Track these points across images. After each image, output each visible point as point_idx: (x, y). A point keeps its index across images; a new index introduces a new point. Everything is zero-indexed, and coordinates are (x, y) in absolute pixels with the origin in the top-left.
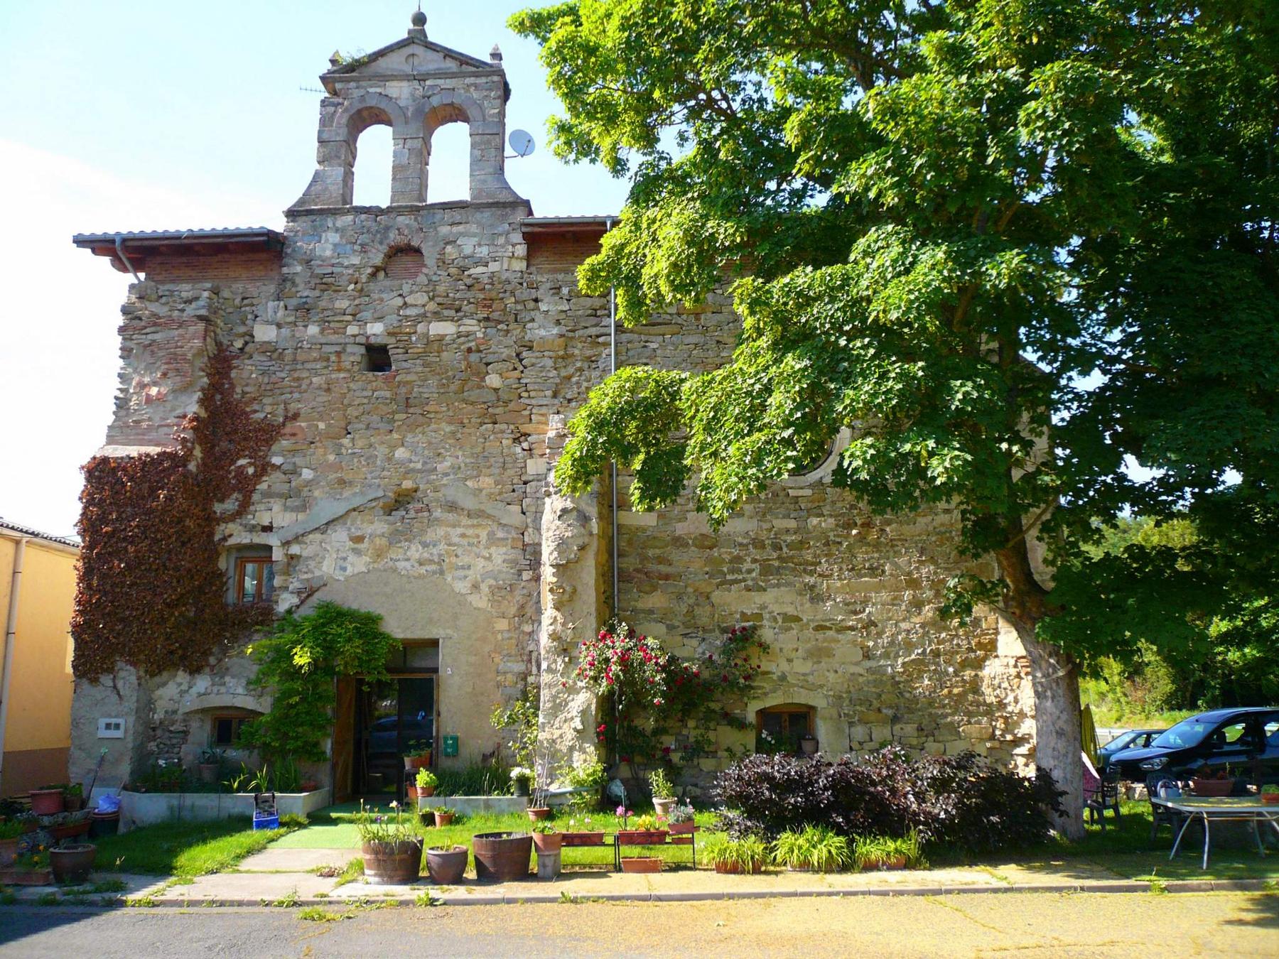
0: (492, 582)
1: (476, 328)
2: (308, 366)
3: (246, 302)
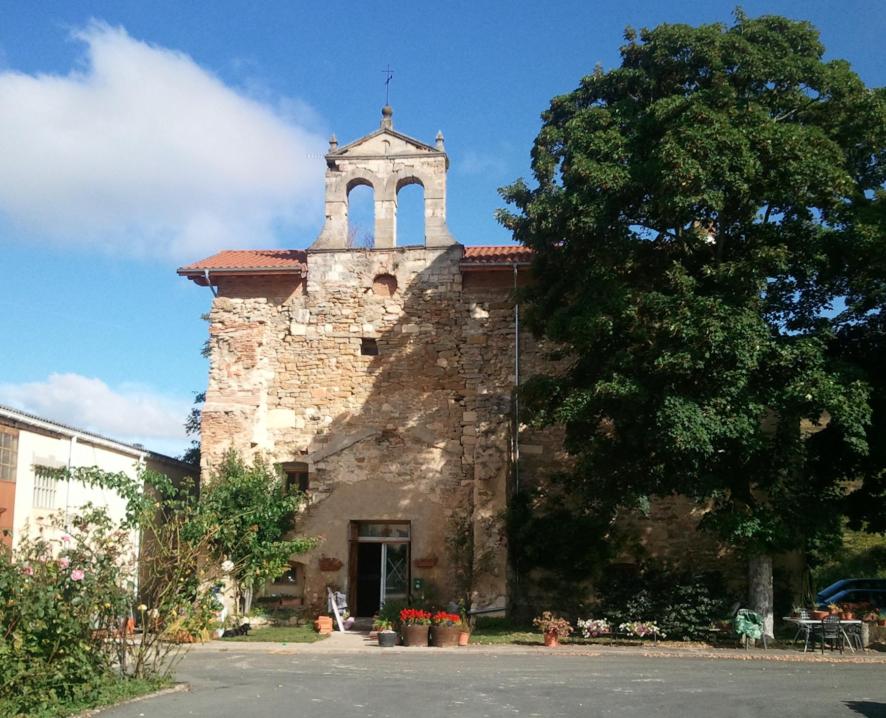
0: (443, 487)
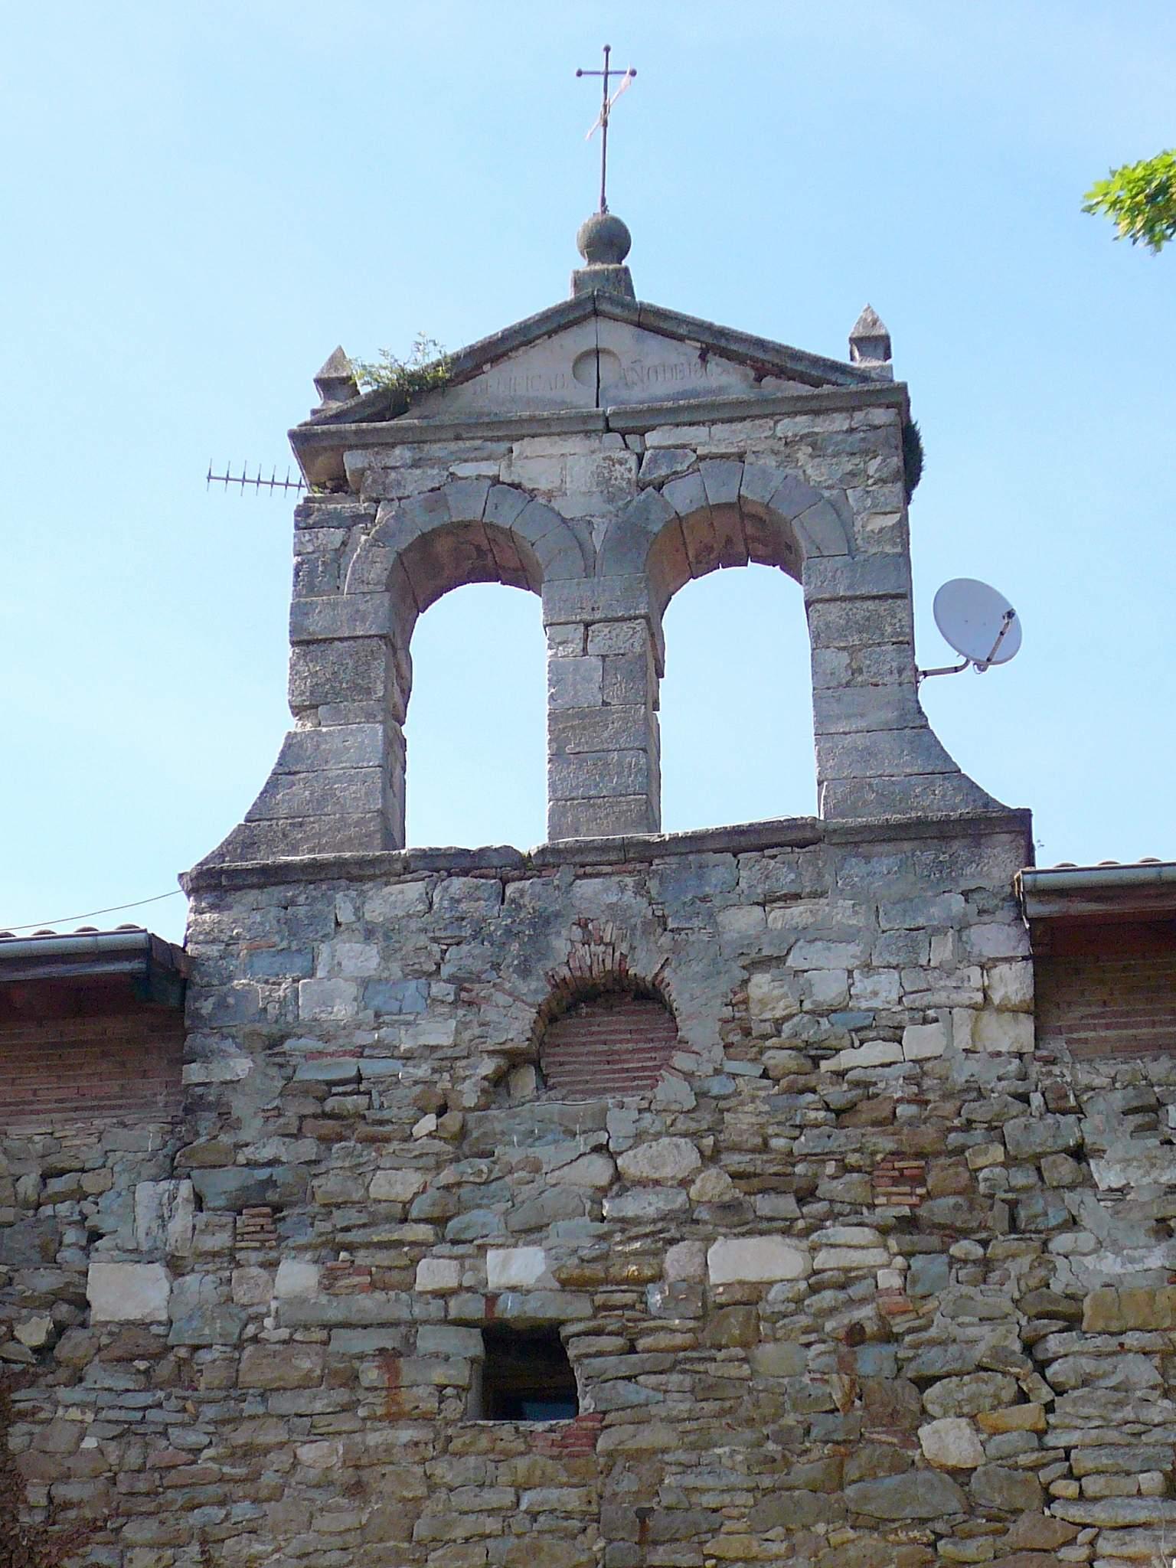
1: (875, 1256)
2: (283, 1403)
3: (56, 1185)
